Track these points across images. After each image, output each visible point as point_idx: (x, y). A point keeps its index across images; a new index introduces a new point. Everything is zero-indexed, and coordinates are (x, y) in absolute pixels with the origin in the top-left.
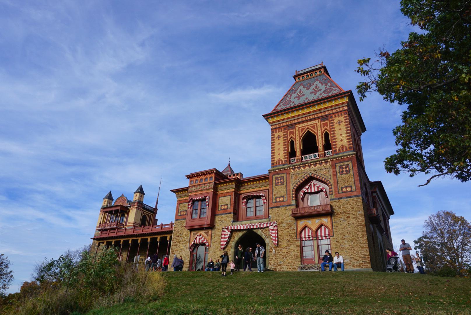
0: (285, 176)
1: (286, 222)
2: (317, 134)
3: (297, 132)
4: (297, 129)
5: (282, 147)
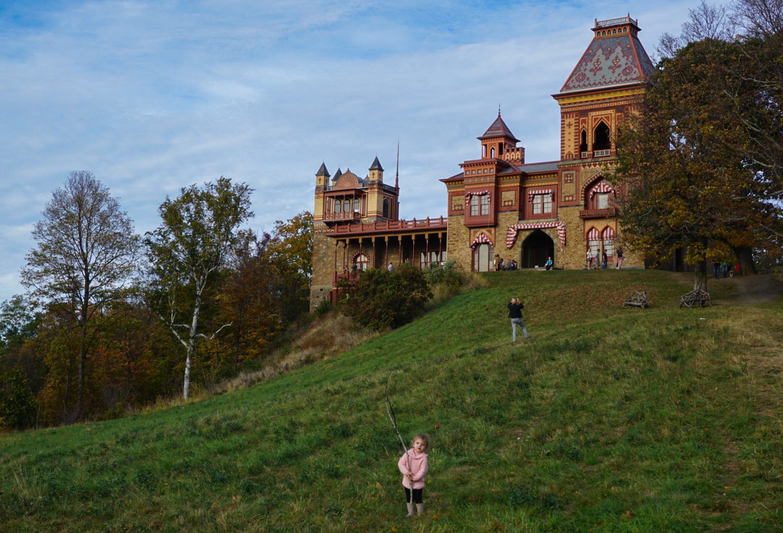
0: (575, 174)
1: (575, 222)
2: (611, 127)
3: (590, 121)
4: (590, 118)
5: (572, 137)
